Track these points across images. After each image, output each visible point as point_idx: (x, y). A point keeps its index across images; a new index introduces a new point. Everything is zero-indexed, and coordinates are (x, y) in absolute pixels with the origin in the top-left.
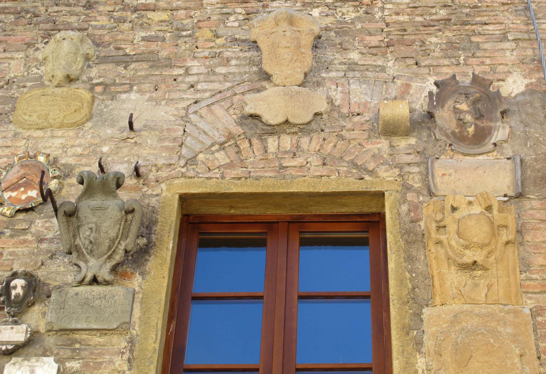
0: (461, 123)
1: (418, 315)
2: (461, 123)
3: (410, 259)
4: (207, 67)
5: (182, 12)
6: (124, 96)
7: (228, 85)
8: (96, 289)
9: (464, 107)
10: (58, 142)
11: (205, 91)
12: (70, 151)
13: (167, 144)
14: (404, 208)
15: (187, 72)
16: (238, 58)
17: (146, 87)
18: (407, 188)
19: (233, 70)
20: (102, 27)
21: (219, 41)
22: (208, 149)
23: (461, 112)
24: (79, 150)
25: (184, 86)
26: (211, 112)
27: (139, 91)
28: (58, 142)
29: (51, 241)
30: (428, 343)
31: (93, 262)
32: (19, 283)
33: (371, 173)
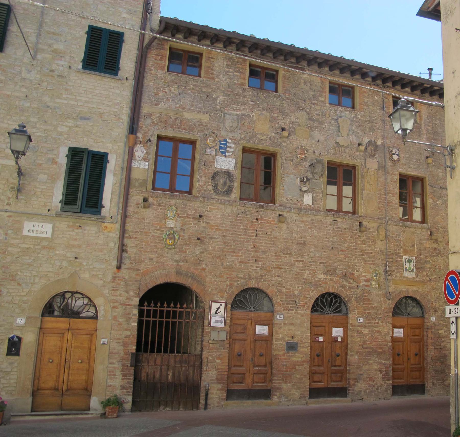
0: (372, 152)
1: (362, 192)
2: (372, 152)
3: (362, 181)
4: (329, 126)
5: (323, 107)
6: (315, 131)
7: (333, 132)
8: (317, 181)
9: (372, 149)
10: (305, 142)
11: (329, 133)
12: (307, 145)
13: (324, 146)
14: (361, 169)
15: (325, 127)
16: (334, 125)
17: (318, 129)
18: (362, 165)
19: (334, 128)
20: (308, 108)
21: (330, 118)
22: (330, 150)
23: (372, 149)
24: (309, 146)
25: (325, 131)
26: (330, 139)
27: (317, 131)
28: (305, 142)
29: (307, 167)
30: (364, 198)
31: (316, 176)
32: (305, 178)
33: (357, 160)
